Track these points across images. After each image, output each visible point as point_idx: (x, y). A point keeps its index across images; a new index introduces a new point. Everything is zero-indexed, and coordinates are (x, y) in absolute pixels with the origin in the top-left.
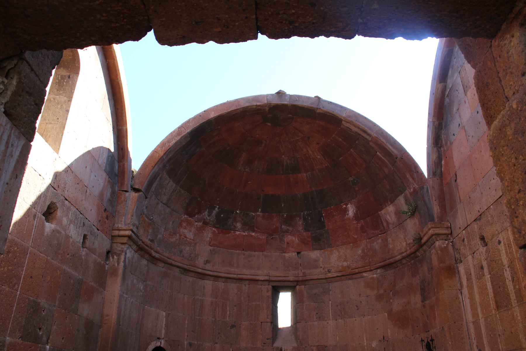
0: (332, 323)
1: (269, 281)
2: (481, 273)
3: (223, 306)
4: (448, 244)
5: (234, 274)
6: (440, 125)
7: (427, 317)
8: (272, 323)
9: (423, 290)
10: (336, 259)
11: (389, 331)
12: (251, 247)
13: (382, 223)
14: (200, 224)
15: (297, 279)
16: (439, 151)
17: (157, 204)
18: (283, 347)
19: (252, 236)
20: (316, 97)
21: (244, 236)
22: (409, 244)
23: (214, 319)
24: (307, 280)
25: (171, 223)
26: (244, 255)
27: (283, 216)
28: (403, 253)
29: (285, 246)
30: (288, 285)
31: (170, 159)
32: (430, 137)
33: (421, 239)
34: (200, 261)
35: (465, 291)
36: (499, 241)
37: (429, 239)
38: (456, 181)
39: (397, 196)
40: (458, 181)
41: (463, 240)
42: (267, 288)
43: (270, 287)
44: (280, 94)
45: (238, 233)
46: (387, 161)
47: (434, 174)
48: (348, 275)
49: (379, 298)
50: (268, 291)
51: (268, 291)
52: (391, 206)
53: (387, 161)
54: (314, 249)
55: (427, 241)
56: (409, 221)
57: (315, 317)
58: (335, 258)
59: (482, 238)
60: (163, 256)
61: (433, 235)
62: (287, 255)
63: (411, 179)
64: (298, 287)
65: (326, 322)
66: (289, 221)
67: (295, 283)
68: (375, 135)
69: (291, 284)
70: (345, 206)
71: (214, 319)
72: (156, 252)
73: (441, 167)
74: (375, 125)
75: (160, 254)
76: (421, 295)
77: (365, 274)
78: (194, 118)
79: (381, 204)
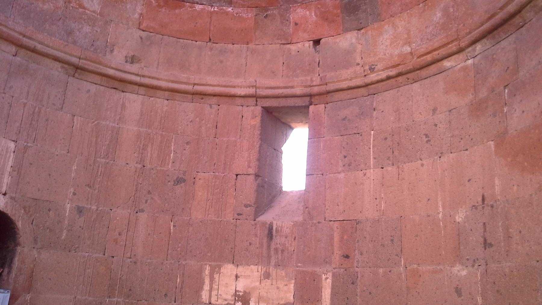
0: (373, 173)
1: (256, 97)
3: (161, 142)
8: (257, 176)
10: (388, 43)
11: (497, 182)
12: (226, 36)
15: (307, 91)
18: (275, 223)
19: (227, 13)
21: (211, 13)
23: (140, 166)
24: (329, 92)
26: (211, 49)
30: (293, 104)
42: (253, 111)
43: (259, 109)
45: (198, 7)
49: (477, 109)
50: (254, 117)
51: (254, 117)
54: (346, 30)
57: (341, 164)
62: (293, 47)
64: (312, 108)
65: (361, 174)
67: (308, 99)
69: (299, 102)
77: (447, 64)
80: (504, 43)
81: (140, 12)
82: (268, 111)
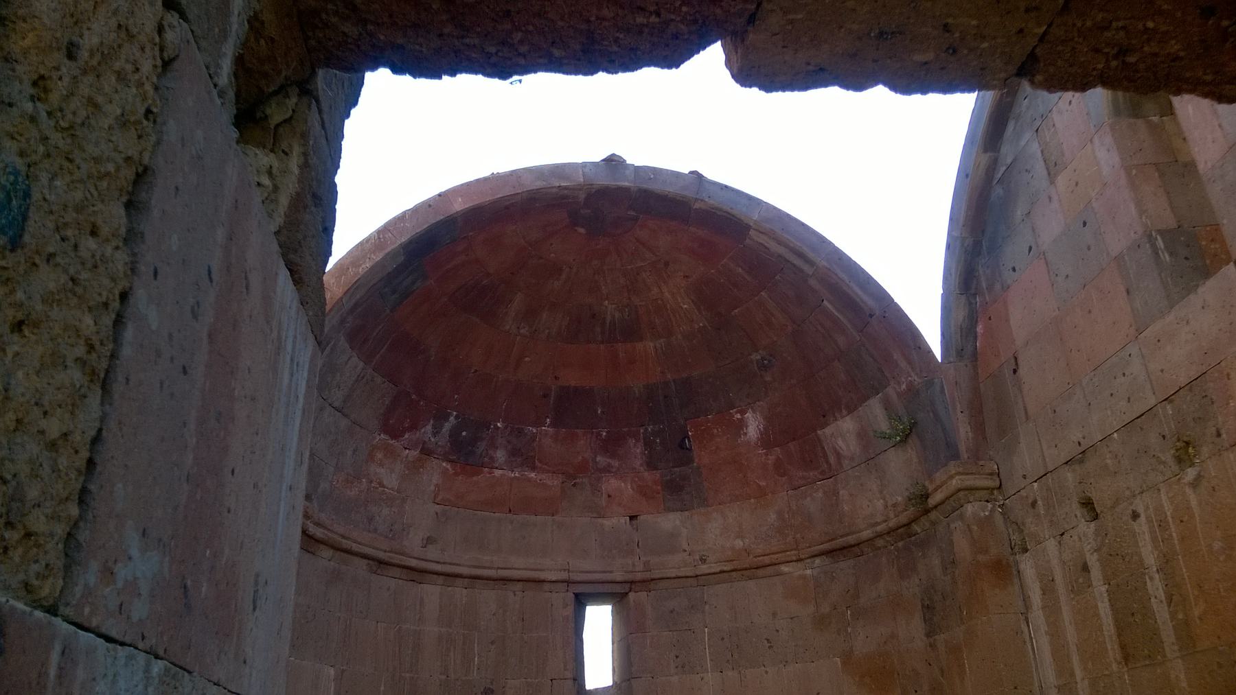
1: (568, 582)
2: (1081, 580)
4: (992, 511)
5: (489, 568)
6: (977, 244)
7: (942, 671)
9: (928, 609)
13: (825, 456)
14: (415, 453)
15: (629, 577)
16: (970, 304)
17: (322, 409)
19: (529, 480)
20: (692, 173)
22: (894, 505)
24: (653, 580)
25: (350, 453)
26: (512, 522)
27: (599, 434)
28: (877, 524)
29: (603, 501)
31: (356, 305)
32: (953, 271)
33: (926, 496)
34: (413, 542)
35: (1038, 616)
36: (1134, 512)
37: (948, 498)
38: (1015, 371)
39: (866, 398)
40: (1021, 371)
41: (1034, 504)
44: (613, 162)
45: (498, 473)
46: (845, 321)
47: (960, 353)
48: (749, 569)
49: (821, 622)
52: (848, 418)
53: (845, 321)
54: (669, 510)
55: (942, 503)
56: (892, 452)
58: (716, 531)
59: (1088, 504)
60: (332, 531)
61: (959, 490)
62: (607, 523)
63: (903, 364)
64: (632, 595)
66: (612, 445)
68: (824, 263)
69: (618, 589)
70: (739, 416)
71: (444, 677)
72: (318, 524)
73: (976, 338)
74: (822, 242)
75: (325, 528)
76: (925, 621)
77: (784, 568)
78: (416, 210)
79: (825, 412)
80: (842, 565)
81: (434, 481)
82: (577, 595)
